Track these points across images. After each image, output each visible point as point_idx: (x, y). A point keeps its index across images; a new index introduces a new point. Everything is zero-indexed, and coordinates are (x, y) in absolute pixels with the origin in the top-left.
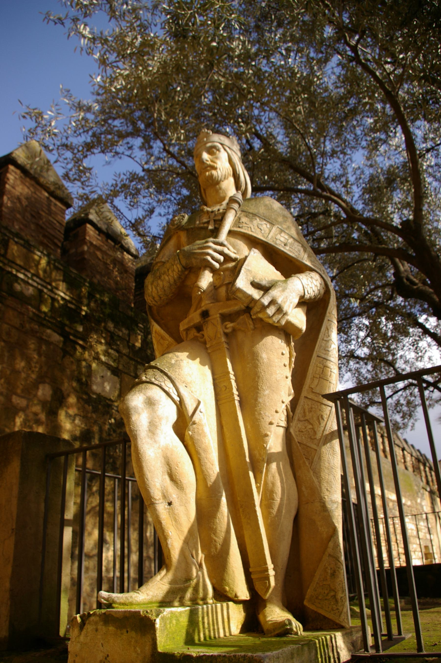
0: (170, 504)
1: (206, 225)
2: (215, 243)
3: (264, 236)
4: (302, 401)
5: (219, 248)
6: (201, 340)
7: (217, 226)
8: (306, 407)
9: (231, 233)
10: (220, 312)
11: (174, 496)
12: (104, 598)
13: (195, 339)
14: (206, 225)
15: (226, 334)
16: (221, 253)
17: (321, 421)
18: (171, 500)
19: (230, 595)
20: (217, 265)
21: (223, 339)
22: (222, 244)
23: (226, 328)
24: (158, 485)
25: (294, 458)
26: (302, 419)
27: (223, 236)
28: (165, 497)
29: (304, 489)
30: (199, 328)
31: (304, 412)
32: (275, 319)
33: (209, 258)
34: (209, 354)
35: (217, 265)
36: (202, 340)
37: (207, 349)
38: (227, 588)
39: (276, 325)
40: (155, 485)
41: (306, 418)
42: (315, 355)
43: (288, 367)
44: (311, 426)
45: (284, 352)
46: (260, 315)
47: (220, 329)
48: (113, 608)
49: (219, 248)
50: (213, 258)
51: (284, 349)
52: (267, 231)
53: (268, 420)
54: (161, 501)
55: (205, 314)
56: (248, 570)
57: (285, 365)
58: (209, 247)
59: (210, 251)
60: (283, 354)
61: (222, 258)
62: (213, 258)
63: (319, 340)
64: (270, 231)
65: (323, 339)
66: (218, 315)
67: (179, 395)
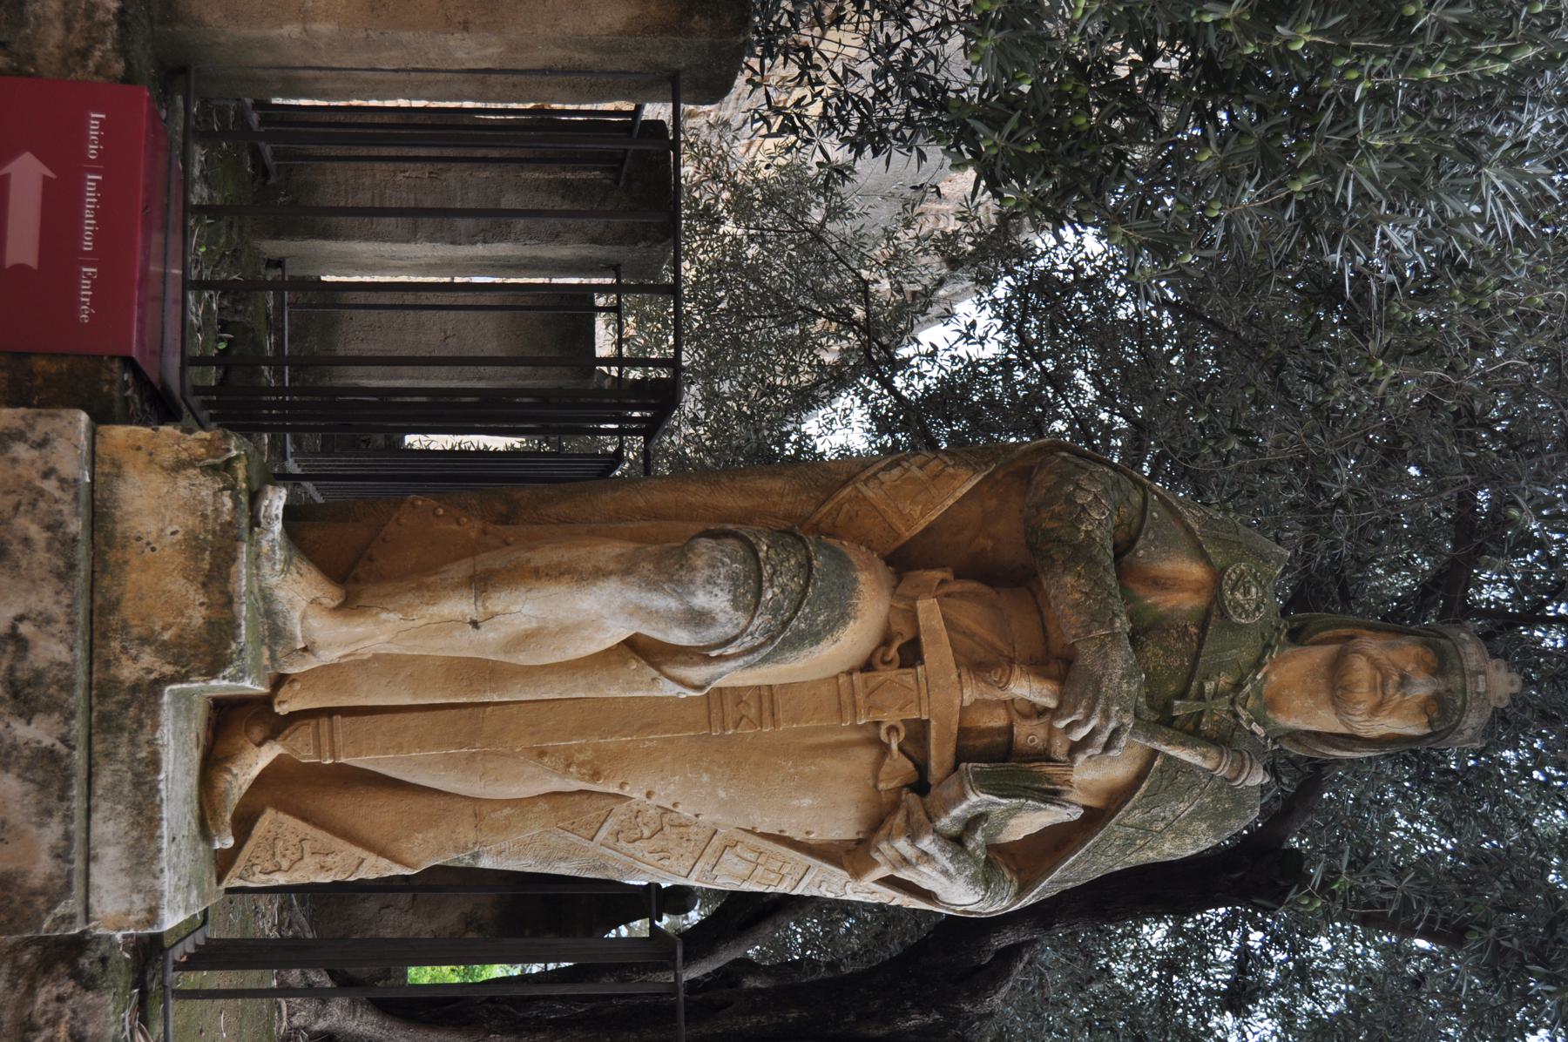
2: (1116, 733)
6: (879, 655)
8: (693, 829)
10: (933, 723)
11: (491, 635)
13: (886, 641)
16: (1087, 742)
17: (657, 856)
19: (282, 690)
29: (507, 811)
31: (681, 825)
34: (836, 677)
36: (877, 661)
37: (850, 673)
40: (516, 603)
41: (667, 829)
44: (647, 833)
47: (890, 718)
53: (656, 789)
54: (481, 609)
58: (1106, 716)
59: (1093, 723)
66: (925, 717)
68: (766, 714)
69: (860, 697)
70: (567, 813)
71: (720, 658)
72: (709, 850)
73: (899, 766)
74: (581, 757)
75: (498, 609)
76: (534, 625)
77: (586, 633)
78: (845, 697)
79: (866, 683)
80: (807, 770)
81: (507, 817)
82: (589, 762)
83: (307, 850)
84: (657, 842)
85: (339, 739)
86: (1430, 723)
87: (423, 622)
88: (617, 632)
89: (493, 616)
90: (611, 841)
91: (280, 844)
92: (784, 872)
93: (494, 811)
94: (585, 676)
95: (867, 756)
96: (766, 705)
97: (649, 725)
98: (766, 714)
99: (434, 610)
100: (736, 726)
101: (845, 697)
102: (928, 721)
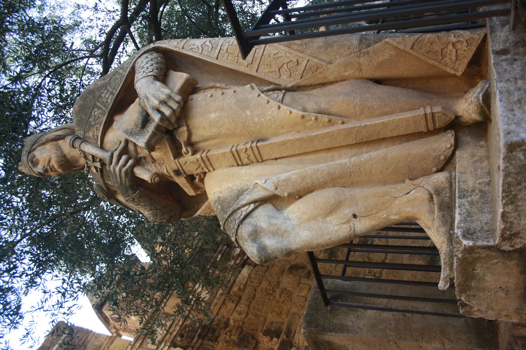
0: (355, 216)
1: (99, 170)
3: (104, 115)
4: (260, 75)
5: (114, 160)
7: (98, 160)
8: (266, 71)
9: (102, 147)
10: (172, 159)
12: (445, 286)
13: (202, 180)
14: (99, 170)
15: (194, 153)
17: (280, 55)
18: (351, 215)
20: (130, 162)
21: (198, 156)
22: (112, 155)
23: (188, 152)
24: (336, 228)
25: (317, 83)
26: (278, 74)
27: (105, 156)
28: (348, 221)
30: (191, 178)
31: (272, 72)
32: (175, 106)
33: (124, 169)
34: (214, 170)
35: (130, 162)
36: (202, 175)
38: (442, 158)
39: (182, 104)
40: (336, 231)
41: (277, 70)
42: (216, 62)
43: (224, 91)
44: (285, 66)
45: (209, 95)
46: (173, 120)
48: (454, 278)
49: (114, 160)
50: (124, 166)
51: (206, 96)
52: (100, 111)
54: (352, 225)
55: (178, 173)
56: (425, 133)
57: (223, 94)
59: (117, 169)
60: (212, 96)
61: (124, 158)
62: (124, 166)
63: (201, 58)
64: (100, 108)
65: (201, 54)
66: (176, 160)
67: (249, 204)
68: (236, 155)
69: (203, 165)
70: (320, 76)
71: (249, 204)
72: (258, 61)
73: (182, 137)
74: (311, 123)
75: (345, 226)
76: (328, 219)
77: (306, 217)
78: (207, 163)
79: (203, 169)
80: (216, 130)
81: (346, 71)
82: (307, 121)
83: (440, 54)
84: (280, 62)
85: (423, 123)
86: (35, 156)
87: (378, 215)
88: (295, 211)
89: (348, 221)
90: (300, 60)
91: (454, 58)
92: (227, 54)
93: (353, 73)
94: (307, 184)
95: (194, 138)
96: (237, 158)
97: (283, 145)
98: (236, 155)
99: (374, 223)
100: (246, 149)
101: (207, 163)
102: (175, 158)
